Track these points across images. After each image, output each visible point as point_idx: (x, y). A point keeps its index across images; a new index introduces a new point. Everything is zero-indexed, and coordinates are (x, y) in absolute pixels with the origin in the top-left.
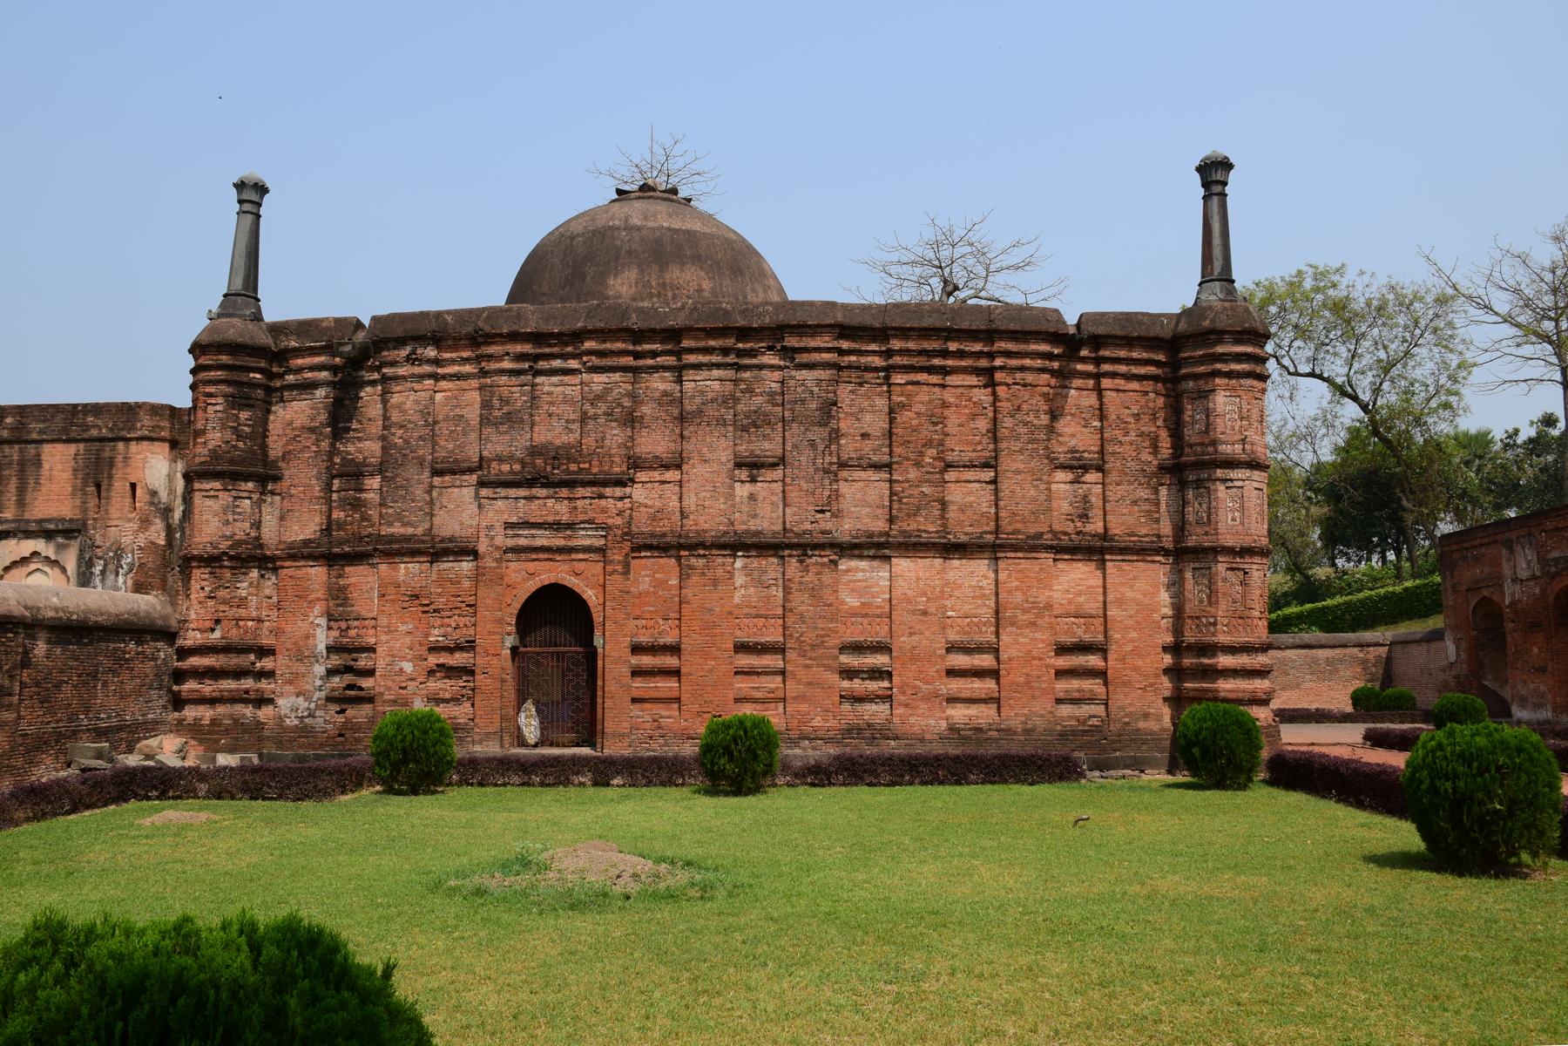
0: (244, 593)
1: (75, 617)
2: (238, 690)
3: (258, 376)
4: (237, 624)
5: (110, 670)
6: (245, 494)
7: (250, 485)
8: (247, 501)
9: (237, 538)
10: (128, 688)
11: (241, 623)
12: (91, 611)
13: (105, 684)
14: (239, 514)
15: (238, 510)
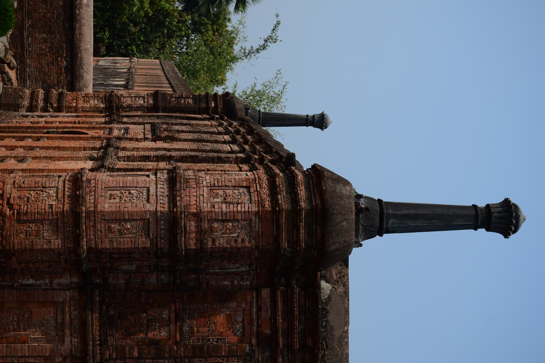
0: (92, 102)
1: (77, 12)
2: (38, 98)
3: (213, 105)
4: (74, 99)
5: (53, 44)
6: (146, 100)
7: (152, 102)
8: (142, 102)
9: (122, 98)
10: (43, 61)
11: (75, 101)
12: (81, 26)
13: (45, 41)
14: (135, 99)
15: (137, 99)
